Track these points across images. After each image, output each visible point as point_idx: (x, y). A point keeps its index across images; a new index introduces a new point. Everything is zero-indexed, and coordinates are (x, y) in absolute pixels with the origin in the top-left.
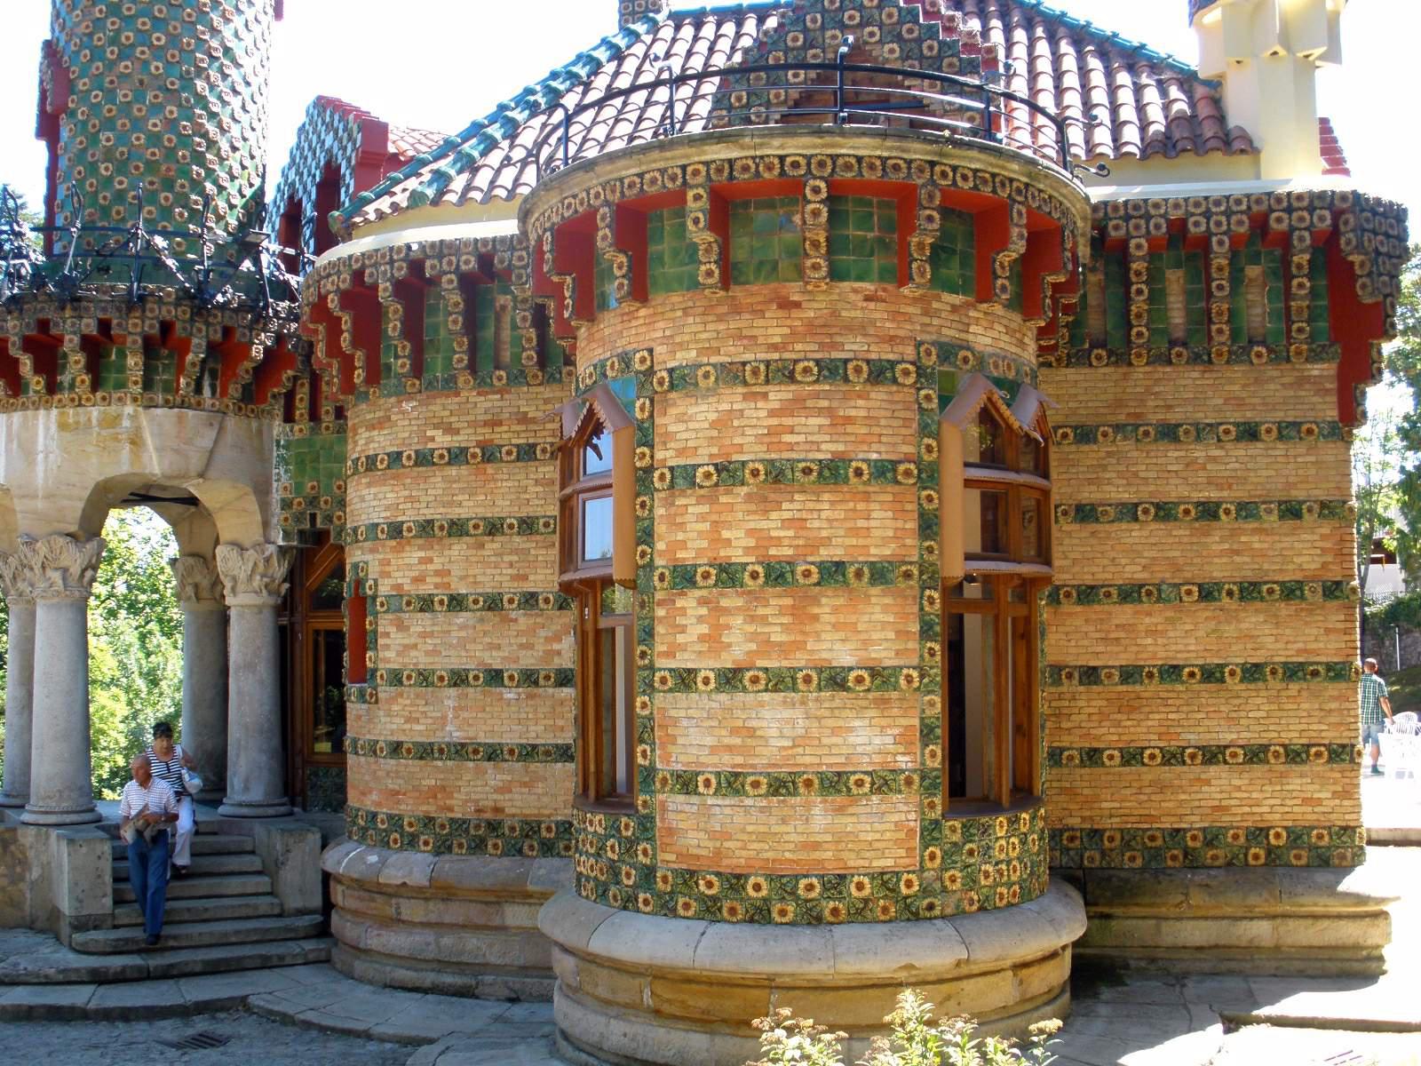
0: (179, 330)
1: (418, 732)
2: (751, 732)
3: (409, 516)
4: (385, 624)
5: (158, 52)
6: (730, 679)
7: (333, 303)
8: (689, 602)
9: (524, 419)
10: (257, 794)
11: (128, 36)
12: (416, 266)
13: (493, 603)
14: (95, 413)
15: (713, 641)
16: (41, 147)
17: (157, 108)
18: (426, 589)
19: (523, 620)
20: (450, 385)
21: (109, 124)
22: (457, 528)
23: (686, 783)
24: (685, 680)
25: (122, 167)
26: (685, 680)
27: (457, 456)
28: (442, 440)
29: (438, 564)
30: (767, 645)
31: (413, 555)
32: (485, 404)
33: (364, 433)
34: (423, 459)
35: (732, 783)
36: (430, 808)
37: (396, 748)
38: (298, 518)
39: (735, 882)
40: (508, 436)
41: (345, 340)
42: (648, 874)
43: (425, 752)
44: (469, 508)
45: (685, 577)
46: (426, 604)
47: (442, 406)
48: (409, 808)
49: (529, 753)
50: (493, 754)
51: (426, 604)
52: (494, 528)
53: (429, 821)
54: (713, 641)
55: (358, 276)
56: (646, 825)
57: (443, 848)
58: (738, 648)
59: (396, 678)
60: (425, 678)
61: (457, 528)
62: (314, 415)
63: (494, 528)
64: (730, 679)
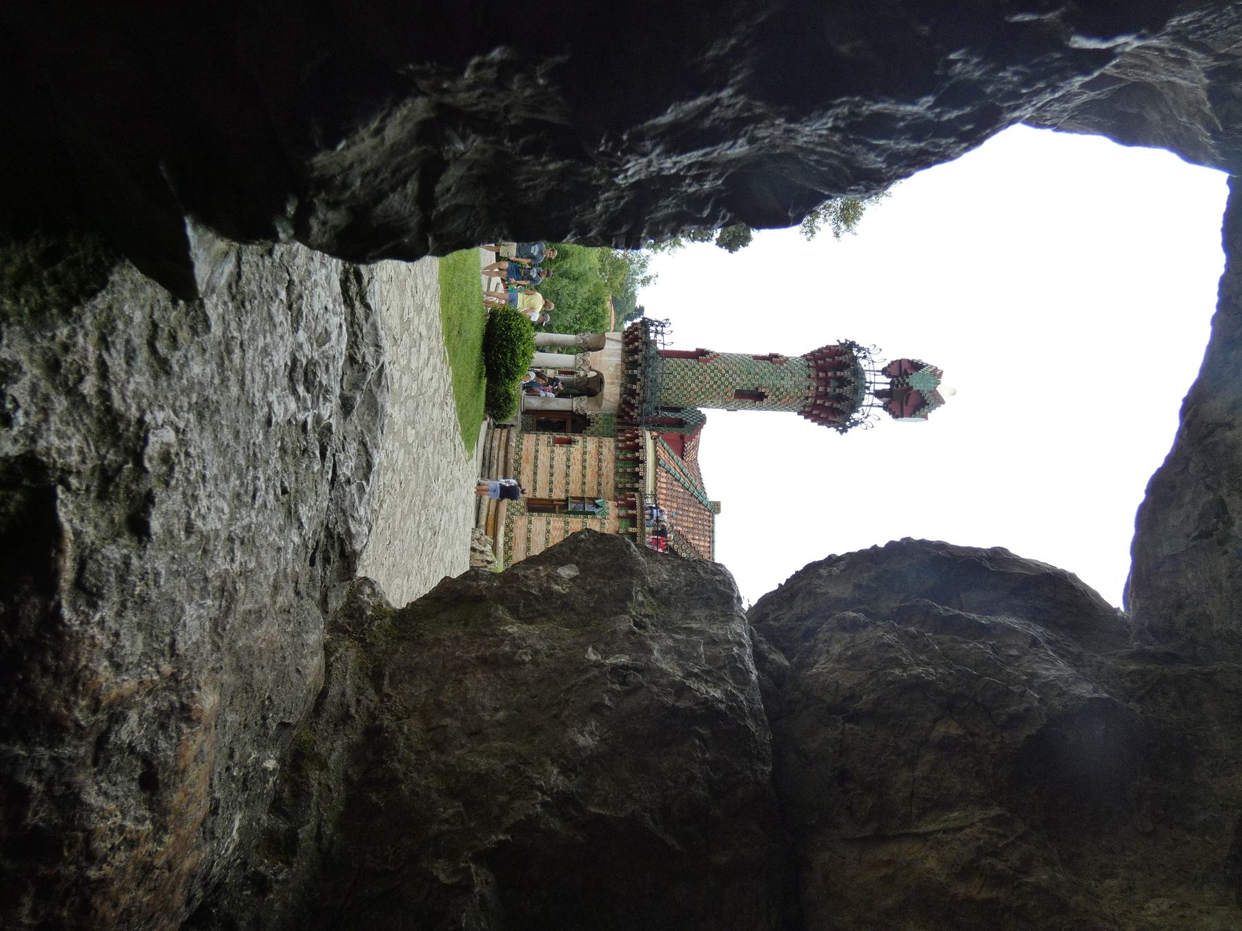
0: (637, 397)
1: (540, 457)
2: (539, 534)
3: (587, 456)
4: (565, 449)
5: (711, 386)
6: (548, 531)
7: (636, 441)
8: (563, 524)
9: (607, 483)
10: (527, 405)
11: (716, 379)
12: (642, 462)
13: (567, 475)
14: (619, 374)
15: (555, 528)
16: (693, 349)
17: (697, 386)
18: (571, 459)
19: (564, 482)
20: (616, 467)
21: (694, 374)
22: (584, 468)
23: (530, 522)
24: (549, 523)
25: (683, 377)
26: (549, 523)
27: (600, 469)
28: (604, 464)
29: (577, 463)
30: (554, 538)
31: (579, 457)
32: (612, 475)
33: (608, 444)
34: (600, 460)
35: (529, 531)
36: (524, 458)
37: (537, 451)
38: (594, 419)
39: (511, 531)
40: (604, 480)
41: (628, 443)
42: (513, 514)
43: (536, 458)
44: (588, 471)
45: (567, 523)
46: (568, 460)
47: (611, 466)
48: (523, 453)
49: (535, 482)
50: (535, 474)
51: (568, 460)
52: (584, 476)
53: (521, 458)
54: (555, 528)
55: (642, 448)
56: (522, 514)
57: (516, 461)
58: (554, 533)
59: (553, 451)
60: (552, 459)
61: (584, 468)
62: (619, 423)
63: (584, 476)
64: (548, 531)
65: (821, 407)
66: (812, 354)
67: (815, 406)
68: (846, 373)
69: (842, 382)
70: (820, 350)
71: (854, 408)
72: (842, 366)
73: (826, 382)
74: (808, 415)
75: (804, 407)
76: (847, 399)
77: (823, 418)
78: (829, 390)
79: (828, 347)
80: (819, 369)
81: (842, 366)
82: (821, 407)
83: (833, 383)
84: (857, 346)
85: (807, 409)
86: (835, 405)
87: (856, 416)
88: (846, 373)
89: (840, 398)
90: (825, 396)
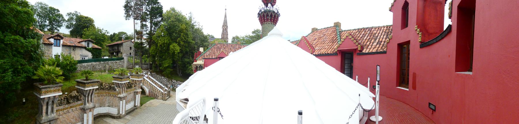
65: (274, 21)
66: (261, 23)
67: (274, 22)
68: (265, 15)
69: (267, 15)
70: (260, 21)
71: (274, 12)
72: (264, 16)
73: (267, 19)
74: (276, 23)
75: (274, 24)
76: (271, 14)
77: (277, 19)
78: (269, 18)
79: (259, 19)
80: (265, 21)
81: (264, 16)
82: (274, 21)
83: (268, 18)
84: (259, 13)
85: (274, 24)
86: (273, 17)
87: (276, 12)
88: (265, 15)
89: (271, 15)
90: (271, 20)
